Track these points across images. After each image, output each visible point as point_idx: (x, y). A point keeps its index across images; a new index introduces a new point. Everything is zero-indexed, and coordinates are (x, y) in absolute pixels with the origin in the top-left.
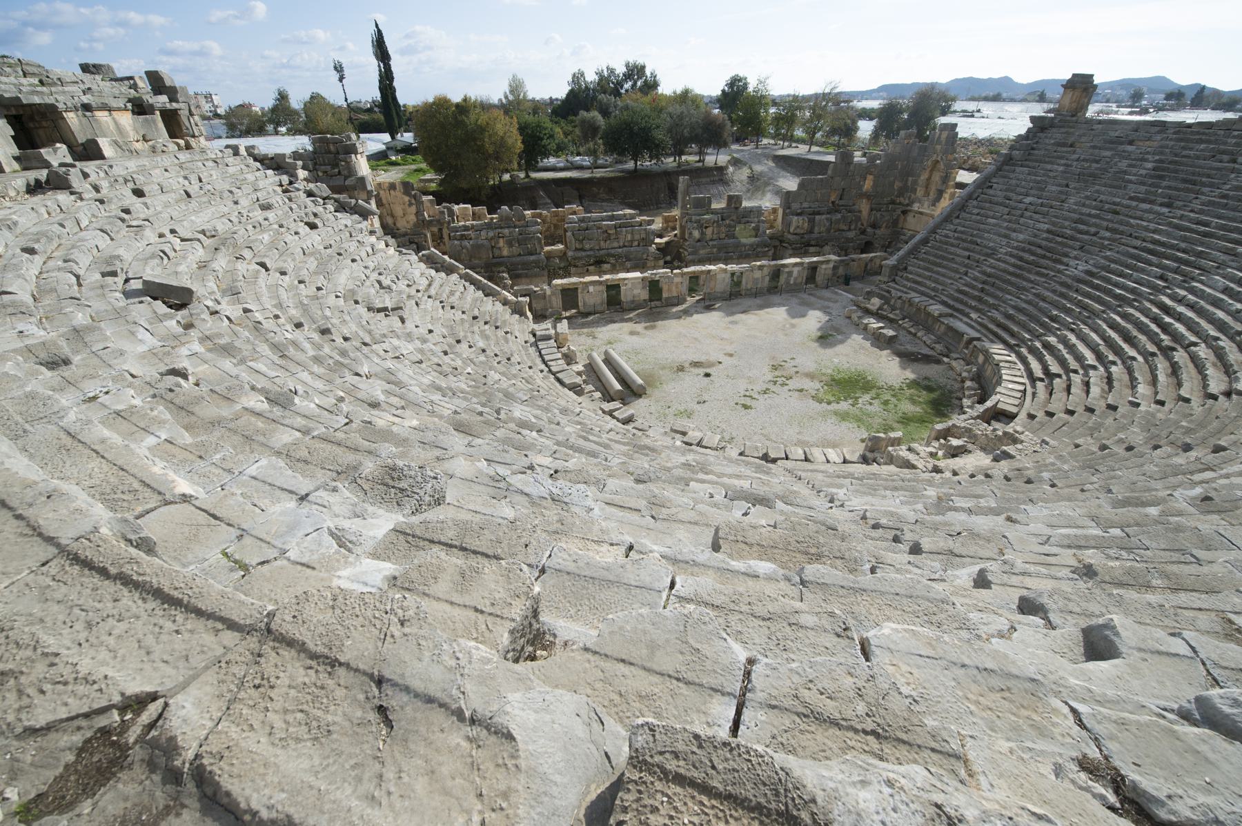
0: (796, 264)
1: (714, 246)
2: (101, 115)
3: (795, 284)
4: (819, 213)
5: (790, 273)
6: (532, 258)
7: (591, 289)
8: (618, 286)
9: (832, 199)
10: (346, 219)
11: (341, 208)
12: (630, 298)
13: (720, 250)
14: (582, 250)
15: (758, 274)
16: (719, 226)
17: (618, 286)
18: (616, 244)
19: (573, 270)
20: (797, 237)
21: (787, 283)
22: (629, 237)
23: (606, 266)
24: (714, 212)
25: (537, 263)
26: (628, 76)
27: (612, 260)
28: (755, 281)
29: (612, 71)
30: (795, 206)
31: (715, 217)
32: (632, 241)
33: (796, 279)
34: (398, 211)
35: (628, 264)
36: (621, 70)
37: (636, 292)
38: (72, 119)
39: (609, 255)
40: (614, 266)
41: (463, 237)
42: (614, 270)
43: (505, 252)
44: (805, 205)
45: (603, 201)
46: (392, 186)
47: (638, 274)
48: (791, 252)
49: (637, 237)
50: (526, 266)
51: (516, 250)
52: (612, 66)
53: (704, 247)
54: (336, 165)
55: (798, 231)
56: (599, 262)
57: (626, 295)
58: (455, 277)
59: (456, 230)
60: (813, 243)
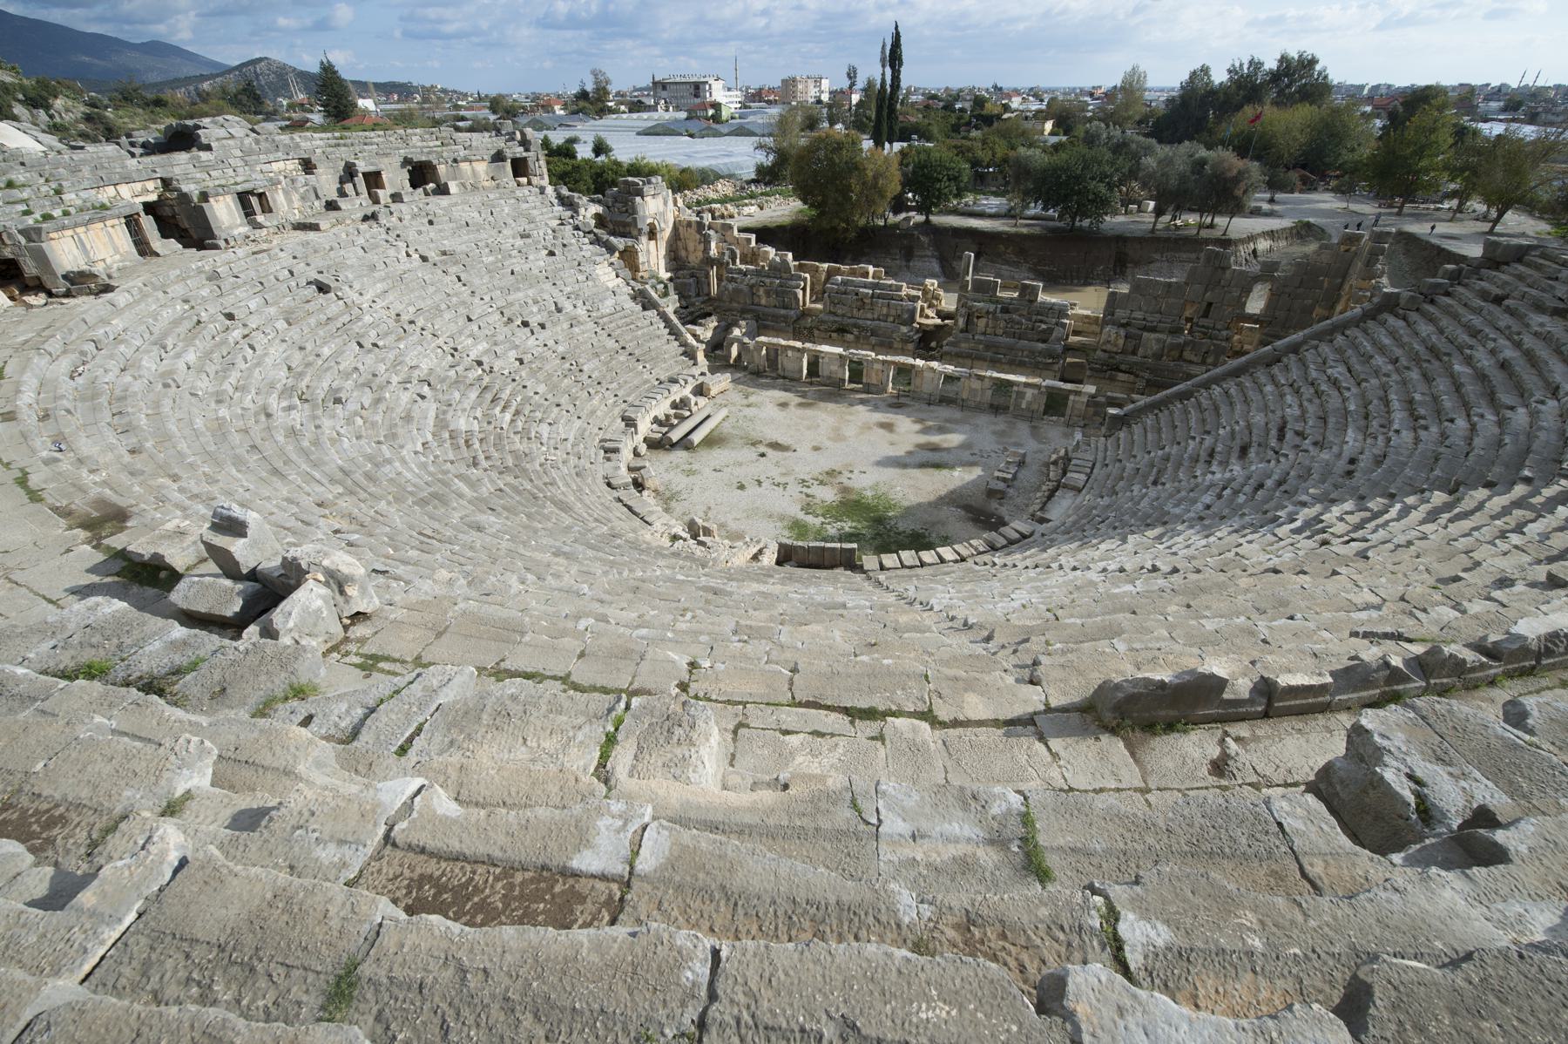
0: (1027, 385)
1: (980, 342)
2: (464, 166)
3: (1028, 408)
4: (1153, 330)
5: (1021, 395)
6: (783, 312)
7: (790, 353)
8: (860, 363)
9: (1187, 314)
10: (589, 250)
11: (597, 241)
12: (826, 373)
13: (988, 347)
14: (835, 314)
15: (976, 385)
16: (995, 319)
17: (817, 357)
18: (869, 316)
19: (816, 332)
20: (1104, 356)
21: (1017, 405)
22: (885, 311)
23: (849, 337)
24: (998, 301)
25: (786, 317)
26: (1275, 76)
27: (856, 331)
28: (973, 391)
29: (1256, 65)
30: (1121, 314)
31: (992, 307)
32: (887, 315)
33: (1029, 403)
34: (691, 248)
35: (873, 340)
36: (1271, 64)
37: (834, 368)
38: (442, 169)
39: (855, 326)
40: (857, 338)
41: (732, 280)
42: (858, 343)
43: (763, 302)
44: (1138, 315)
45: (1007, 262)
46: (689, 224)
47: (839, 350)
48: (1088, 373)
49: (893, 312)
50: (776, 318)
51: (773, 300)
52: (1258, 56)
53: (967, 340)
54: (626, 204)
55: (1108, 347)
56: (842, 330)
57: (826, 368)
58: (652, 313)
59: (731, 271)
60: (1123, 367)
